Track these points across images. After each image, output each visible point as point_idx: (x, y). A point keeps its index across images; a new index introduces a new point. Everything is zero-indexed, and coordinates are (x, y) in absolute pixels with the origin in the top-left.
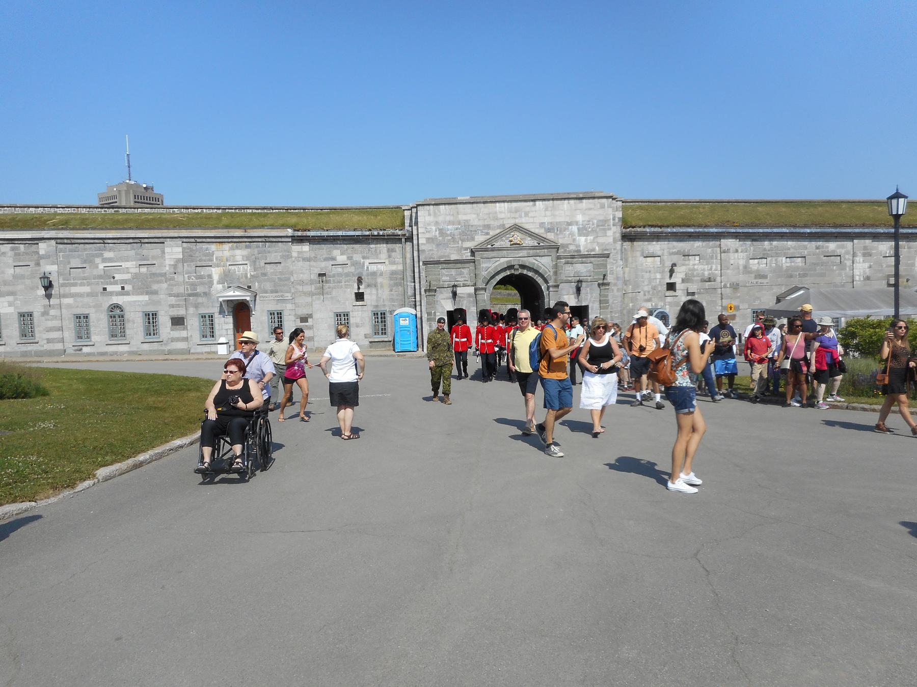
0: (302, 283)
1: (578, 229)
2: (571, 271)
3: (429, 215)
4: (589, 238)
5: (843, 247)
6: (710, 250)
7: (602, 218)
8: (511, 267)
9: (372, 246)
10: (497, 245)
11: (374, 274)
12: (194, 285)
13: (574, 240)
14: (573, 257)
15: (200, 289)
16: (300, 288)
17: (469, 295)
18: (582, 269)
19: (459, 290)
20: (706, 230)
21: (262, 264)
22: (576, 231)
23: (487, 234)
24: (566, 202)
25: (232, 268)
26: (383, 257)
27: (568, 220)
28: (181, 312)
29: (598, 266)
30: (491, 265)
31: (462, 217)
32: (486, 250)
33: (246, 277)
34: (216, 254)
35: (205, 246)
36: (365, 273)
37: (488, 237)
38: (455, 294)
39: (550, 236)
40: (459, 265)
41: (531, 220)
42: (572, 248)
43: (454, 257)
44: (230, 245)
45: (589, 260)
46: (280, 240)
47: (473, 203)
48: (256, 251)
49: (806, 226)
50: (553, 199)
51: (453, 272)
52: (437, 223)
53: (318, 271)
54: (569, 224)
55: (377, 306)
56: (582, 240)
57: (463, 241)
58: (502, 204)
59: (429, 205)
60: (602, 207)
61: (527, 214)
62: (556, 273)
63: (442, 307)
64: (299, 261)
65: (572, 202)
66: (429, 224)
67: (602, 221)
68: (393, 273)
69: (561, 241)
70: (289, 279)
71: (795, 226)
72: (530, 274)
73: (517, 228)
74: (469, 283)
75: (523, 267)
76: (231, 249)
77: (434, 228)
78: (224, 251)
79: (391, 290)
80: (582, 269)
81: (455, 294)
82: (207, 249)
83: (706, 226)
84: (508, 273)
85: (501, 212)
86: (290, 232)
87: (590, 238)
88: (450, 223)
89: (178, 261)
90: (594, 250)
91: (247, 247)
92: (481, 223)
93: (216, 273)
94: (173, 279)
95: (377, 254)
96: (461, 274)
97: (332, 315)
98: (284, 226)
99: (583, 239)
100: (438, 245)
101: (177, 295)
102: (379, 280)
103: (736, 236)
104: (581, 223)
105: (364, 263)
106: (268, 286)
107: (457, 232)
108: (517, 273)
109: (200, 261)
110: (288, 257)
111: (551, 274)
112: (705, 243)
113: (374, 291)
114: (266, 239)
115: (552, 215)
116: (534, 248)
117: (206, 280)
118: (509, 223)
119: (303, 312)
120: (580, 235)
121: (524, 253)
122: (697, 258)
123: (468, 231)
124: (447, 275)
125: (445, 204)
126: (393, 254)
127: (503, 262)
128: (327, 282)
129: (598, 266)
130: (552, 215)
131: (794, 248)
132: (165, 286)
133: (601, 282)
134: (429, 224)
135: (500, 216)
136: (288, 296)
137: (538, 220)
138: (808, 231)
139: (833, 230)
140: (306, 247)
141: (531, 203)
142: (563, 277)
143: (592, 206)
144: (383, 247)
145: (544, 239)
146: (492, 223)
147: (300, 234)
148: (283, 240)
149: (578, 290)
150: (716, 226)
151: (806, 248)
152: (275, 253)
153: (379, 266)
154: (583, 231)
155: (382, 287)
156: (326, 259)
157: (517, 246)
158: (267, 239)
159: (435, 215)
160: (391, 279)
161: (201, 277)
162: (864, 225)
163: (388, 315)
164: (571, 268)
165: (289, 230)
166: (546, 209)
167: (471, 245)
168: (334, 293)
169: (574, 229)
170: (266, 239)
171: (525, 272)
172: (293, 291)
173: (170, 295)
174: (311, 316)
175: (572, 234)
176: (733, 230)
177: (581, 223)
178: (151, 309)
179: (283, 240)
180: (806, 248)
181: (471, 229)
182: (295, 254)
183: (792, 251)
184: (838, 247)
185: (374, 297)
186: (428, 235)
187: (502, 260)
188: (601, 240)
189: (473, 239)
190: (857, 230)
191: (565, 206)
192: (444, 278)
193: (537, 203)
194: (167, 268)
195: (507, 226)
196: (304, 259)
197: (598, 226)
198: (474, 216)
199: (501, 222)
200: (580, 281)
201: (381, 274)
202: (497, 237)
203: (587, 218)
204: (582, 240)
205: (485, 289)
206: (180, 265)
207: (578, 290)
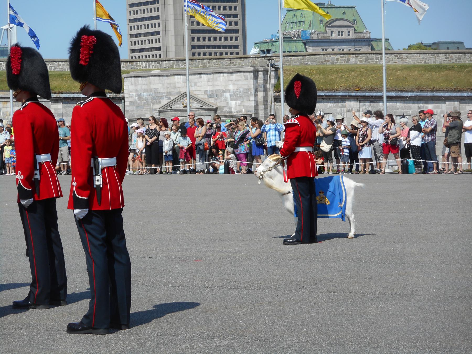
1: (230, 95)
3: (132, 84)
5: (438, 108)
6: (339, 110)
7: (246, 87)
10: (174, 107)
13: (228, 103)
20: (334, 94)
22: (229, 96)
23: (169, 98)
24: (222, 75)
27: (223, 88)
31: (153, 86)
32: (167, 111)
37: (170, 101)
39: (211, 101)
41: (198, 89)
42: (226, 109)
47: (160, 76)
49: (410, 91)
50: (213, 73)
52: (136, 91)
54: (224, 92)
56: (233, 104)
57: (153, 104)
58: (179, 77)
59: (131, 77)
60: (246, 78)
61: (195, 85)
65: (226, 75)
66: (131, 92)
67: (247, 89)
69: (219, 105)
71: (401, 91)
73: (184, 95)
77: (134, 94)
83: (336, 91)
85: (178, 83)
87: (238, 102)
88: (145, 90)
90: (241, 111)
92: (165, 91)
99: (233, 103)
100: (137, 107)
103: (357, 98)
104: (232, 91)
107: (149, 98)
112: (335, 104)
115: (213, 85)
118: (183, 90)
120: (232, 100)
122: (330, 115)
123: (156, 97)
125: (141, 77)
130: (213, 85)
131: (402, 108)
134: (131, 92)
135: (178, 85)
137: (203, 89)
138: (410, 94)
139: (429, 94)
141: (198, 76)
143: (240, 78)
145: (205, 104)
146: (172, 90)
150: (345, 90)
151: (411, 108)
154: (234, 97)
159: (136, 85)
162: (455, 90)
166: (209, 81)
167: (157, 106)
169: (228, 95)
175: (226, 99)
176: (353, 94)
177: (232, 91)
180: (411, 108)
183: (400, 110)
184: (435, 108)
186: (131, 100)
188: (246, 104)
189: (160, 103)
190: (447, 94)
191: (221, 78)
193: (203, 76)
195: (182, 93)
197: (244, 93)
198: (161, 85)
199: (179, 91)
202: (174, 101)
203: (236, 88)
204: (233, 104)
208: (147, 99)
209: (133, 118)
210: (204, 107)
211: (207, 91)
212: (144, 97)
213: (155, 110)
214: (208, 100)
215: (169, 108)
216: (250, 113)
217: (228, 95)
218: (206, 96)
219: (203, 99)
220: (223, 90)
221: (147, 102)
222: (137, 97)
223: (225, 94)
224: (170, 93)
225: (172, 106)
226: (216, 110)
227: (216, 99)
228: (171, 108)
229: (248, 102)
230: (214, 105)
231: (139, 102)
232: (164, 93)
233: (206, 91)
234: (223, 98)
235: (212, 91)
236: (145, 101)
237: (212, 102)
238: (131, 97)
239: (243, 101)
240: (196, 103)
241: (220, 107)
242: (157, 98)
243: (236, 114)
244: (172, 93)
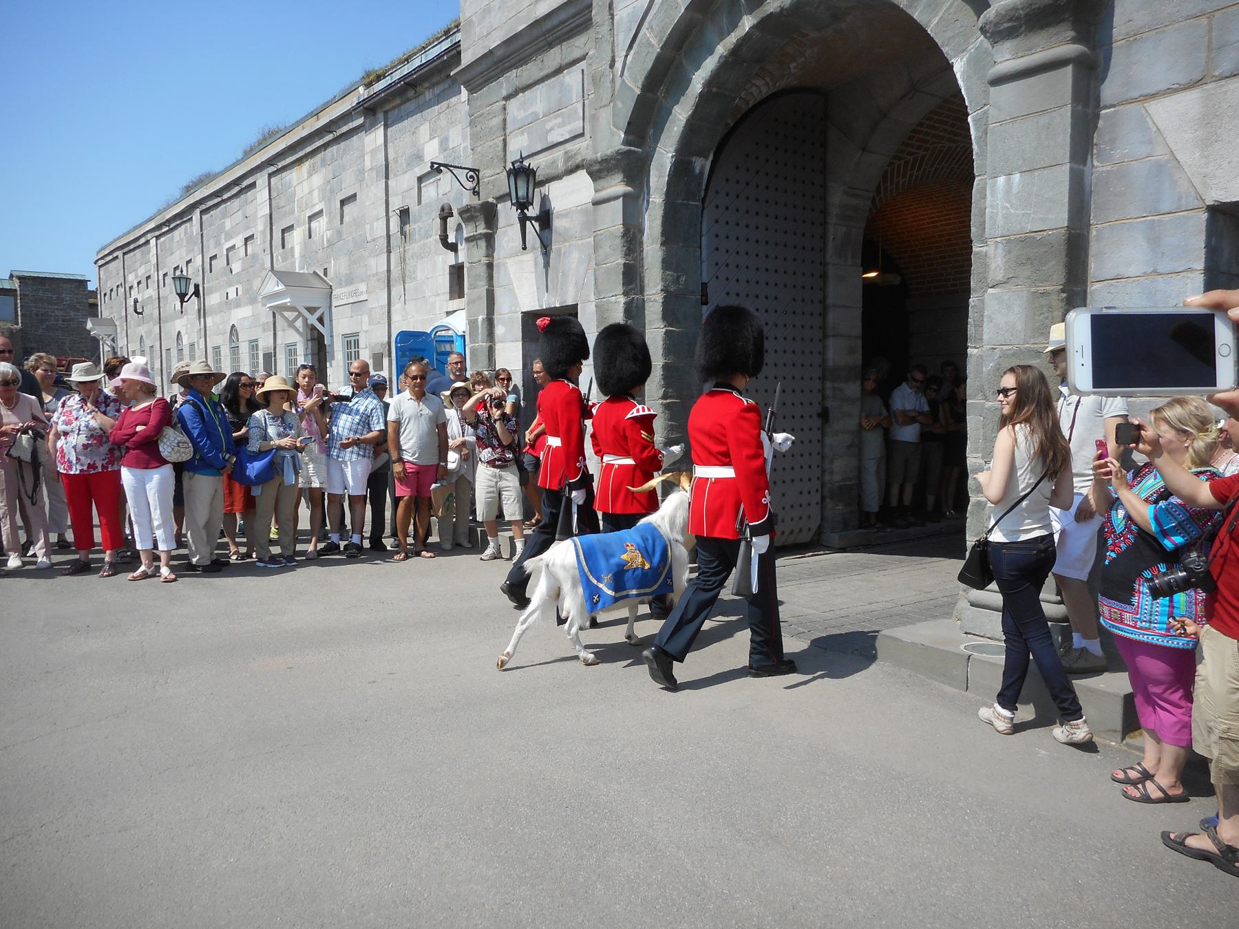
205: (632, 165)
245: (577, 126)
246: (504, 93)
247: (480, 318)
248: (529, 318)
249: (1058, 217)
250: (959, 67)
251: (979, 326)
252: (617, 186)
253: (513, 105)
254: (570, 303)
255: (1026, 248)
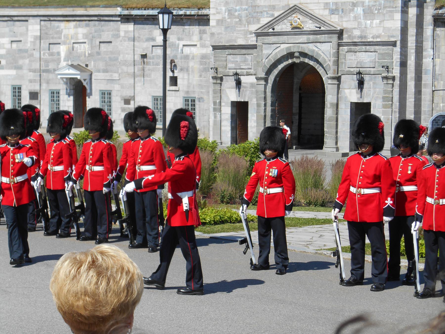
0: (125, 63)
1: (364, 10)
2: (354, 60)
4: (375, 22)
8: (291, 55)
9: (186, 27)
10: (278, 28)
11: (187, 57)
12: (47, 62)
13: (360, 23)
14: (355, 44)
15: (51, 66)
16: (125, 68)
17: (252, 85)
18: (365, 58)
19: (244, 79)
21: (98, 43)
22: (362, 12)
23: (273, 15)
25: (76, 45)
26: (195, 39)
28: (36, 87)
29: (383, 56)
30: (273, 50)
32: (267, 34)
33: (85, 56)
34: (65, 32)
35: (56, 24)
36: (179, 56)
38: (239, 83)
40: (244, 51)
43: (241, 42)
44: (74, 23)
45: (372, 48)
46: (111, 19)
48: (93, 29)
51: (238, 58)
53: (139, 52)
54: (354, 5)
55: (187, 92)
57: (249, 23)
62: (337, 63)
63: (228, 96)
64: (125, 41)
68: (204, 57)
69: (345, 25)
70: (117, 59)
72: (312, 63)
74: (252, 71)
75: (303, 54)
76: (76, 27)
77: (224, 9)
78: (69, 29)
79: (201, 76)
80: (365, 58)
81: (239, 83)
82: (58, 27)
84: (290, 61)
86: (118, 11)
89: (35, 38)
91: (87, 26)
93: (63, 50)
94: (32, 55)
95: (190, 36)
96: (245, 61)
97: (150, 99)
98: (117, 6)
100: (226, 28)
101: (34, 71)
102: (191, 64)
105: (178, 45)
106: (101, 65)
107: (244, 14)
108: (297, 61)
109: (53, 38)
110: (118, 36)
111: (331, 64)
113: (186, 77)
114: (100, 18)
116: (314, 33)
117: (56, 57)
119: (128, 93)
120: (365, 18)
121: (303, 38)
124: (232, 62)
126: (204, 36)
127: (282, 49)
128: (148, 64)
129: (383, 56)
132: (27, 61)
133: (384, 75)
136: (116, 76)
140: (130, 27)
142: (343, 68)
144: (196, 29)
145: (324, 23)
147: (126, 12)
148: (114, 19)
149: (361, 84)
152: (107, 31)
153: (192, 48)
155: (193, 71)
156: (148, 40)
157: (297, 30)
158: (102, 18)
160: (201, 63)
161: (52, 54)
163: (197, 102)
164: (353, 57)
165: (119, 9)
167: (254, 27)
168: (153, 76)
169: (359, 10)
170: (100, 18)
171: (306, 60)
172: (120, 71)
173: (30, 70)
174: (134, 98)
178: (17, 83)
179: (114, 19)
181: (257, 10)
182: (122, 34)
185: (186, 82)
186: (219, 17)
187: (283, 46)
188: (388, 24)
189: (258, 21)
192: (230, 65)
194: (29, 45)
195: (291, 6)
196: (129, 39)
200: (359, 73)
201: (193, 58)
205: (266, 80)
206: (38, 41)
207: (361, 84)
208: (241, 17)
209: (220, 44)
210: (322, 28)
211: (330, 3)
212: (237, 14)
213: (251, 33)
214: (329, 19)
215: (271, 30)
216: (393, 39)
217: (359, 10)
218: (327, 12)
219: (322, 16)
220: (353, 3)
221: (240, 20)
222: (227, 14)
223: (356, 8)
224: (273, 8)
225: (276, 27)
226: (340, 33)
227: (342, 17)
228: (274, 29)
229: (392, 21)
230: (339, 25)
231: (229, 20)
232: (265, 6)
233: (327, 4)
234: (352, 15)
235: (336, 4)
236: (237, 20)
237: (336, 22)
238: (218, 13)
239: (383, 21)
240: (311, 22)
241: (346, 28)
242: (255, 15)
243: (371, 40)
244: (277, 7)
245: (250, 67)
246: (227, 53)
247: (218, 101)
248: (233, 103)
249: (335, 101)
250: (324, 79)
251: (326, 112)
252: (263, 82)
253: (229, 56)
254: (246, 101)
255: (332, 104)
